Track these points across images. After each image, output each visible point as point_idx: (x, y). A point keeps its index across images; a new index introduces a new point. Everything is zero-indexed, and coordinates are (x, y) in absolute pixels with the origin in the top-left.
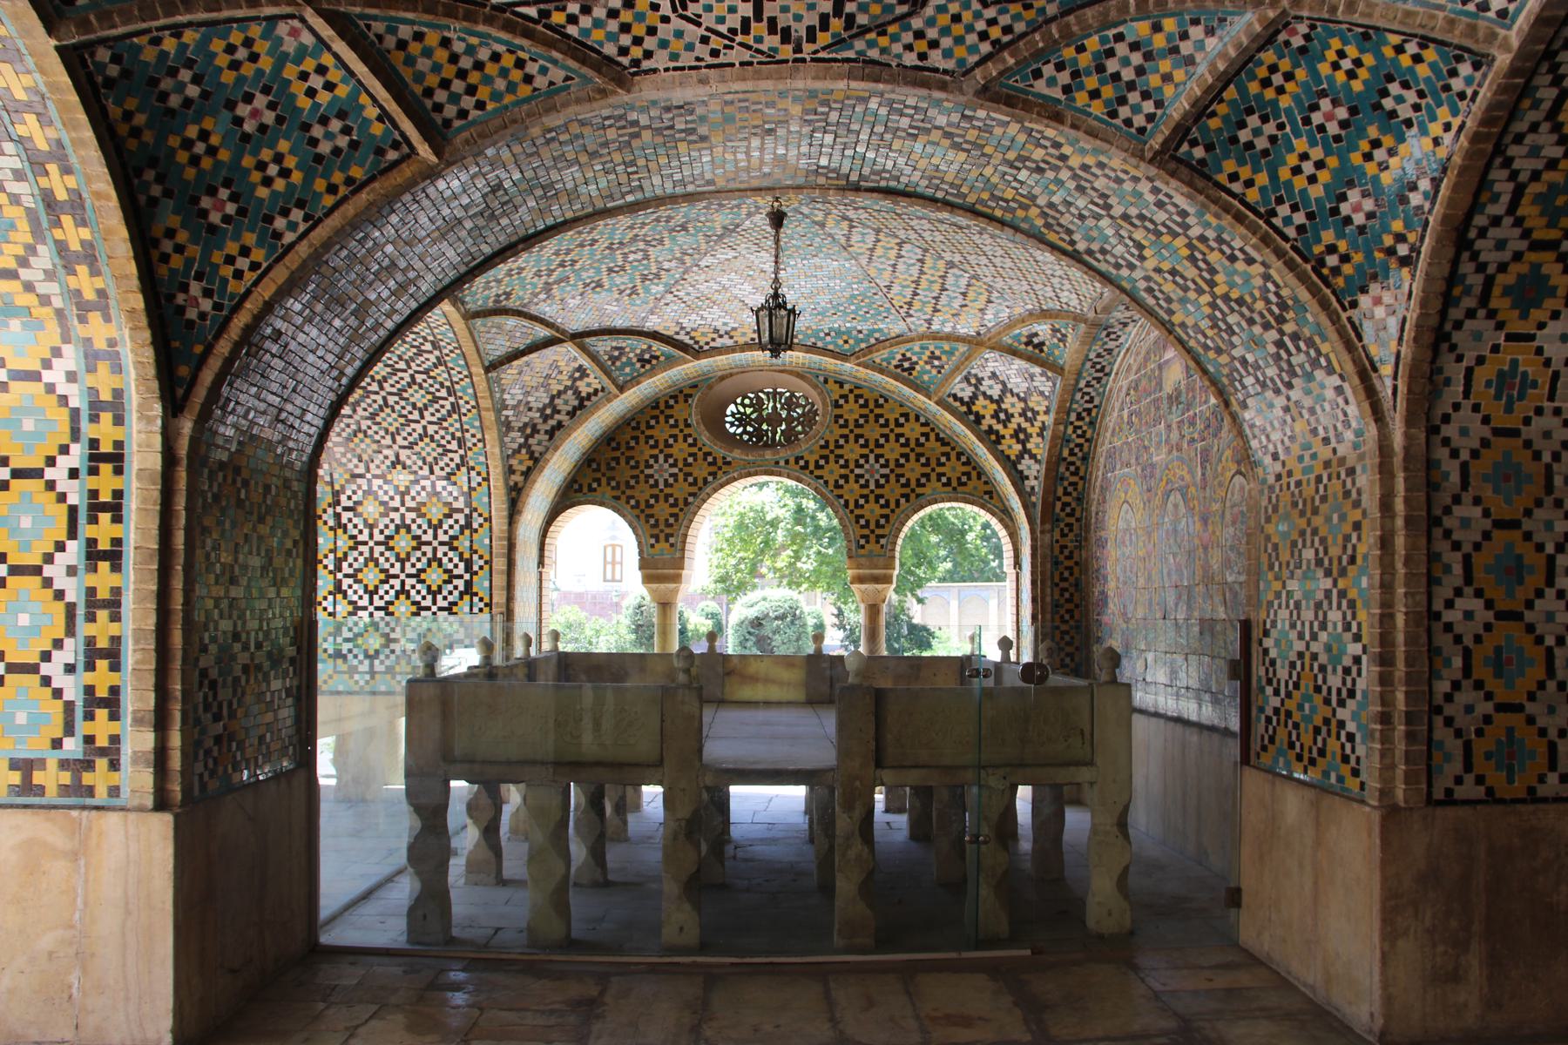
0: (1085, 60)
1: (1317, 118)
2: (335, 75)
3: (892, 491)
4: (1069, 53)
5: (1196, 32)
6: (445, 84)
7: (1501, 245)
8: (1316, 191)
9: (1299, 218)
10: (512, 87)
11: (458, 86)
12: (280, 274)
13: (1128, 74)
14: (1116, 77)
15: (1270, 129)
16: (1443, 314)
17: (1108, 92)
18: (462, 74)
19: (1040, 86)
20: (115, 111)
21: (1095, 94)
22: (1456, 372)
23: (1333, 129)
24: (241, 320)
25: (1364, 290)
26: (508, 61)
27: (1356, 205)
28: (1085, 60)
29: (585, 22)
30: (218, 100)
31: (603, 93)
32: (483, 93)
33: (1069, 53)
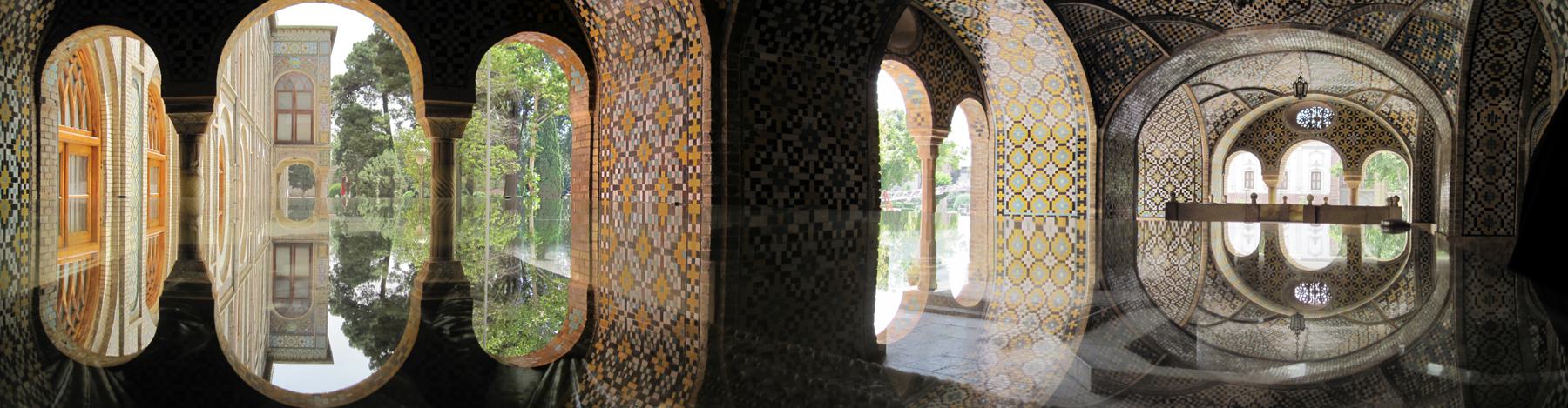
0: (1361, 22)
1: (1428, 41)
2: (1140, 38)
3: (1361, 146)
4: (1356, 20)
5: (1391, 16)
6: (1171, 36)
7: (1482, 79)
8: (1431, 61)
9: (1428, 68)
10: (1190, 35)
11: (1174, 36)
12: (1127, 89)
13: (1374, 26)
14: (1370, 27)
15: (1416, 42)
16: (1468, 98)
17: (1369, 31)
18: (1176, 33)
19: (1348, 29)
20: (1085, 55)
21: (1365, 31)
22: (1475, 114)
23: (1433, 44)
24: (1116, 102)
25: (1447, 89)
26: (1188, 29)
27: (1442, 66)
28: (1361, 22)
29: (1210, 17)
30: (1109, 48)
31: (1217, 35)
32: (1182, 38)
33: (1356, 20)
